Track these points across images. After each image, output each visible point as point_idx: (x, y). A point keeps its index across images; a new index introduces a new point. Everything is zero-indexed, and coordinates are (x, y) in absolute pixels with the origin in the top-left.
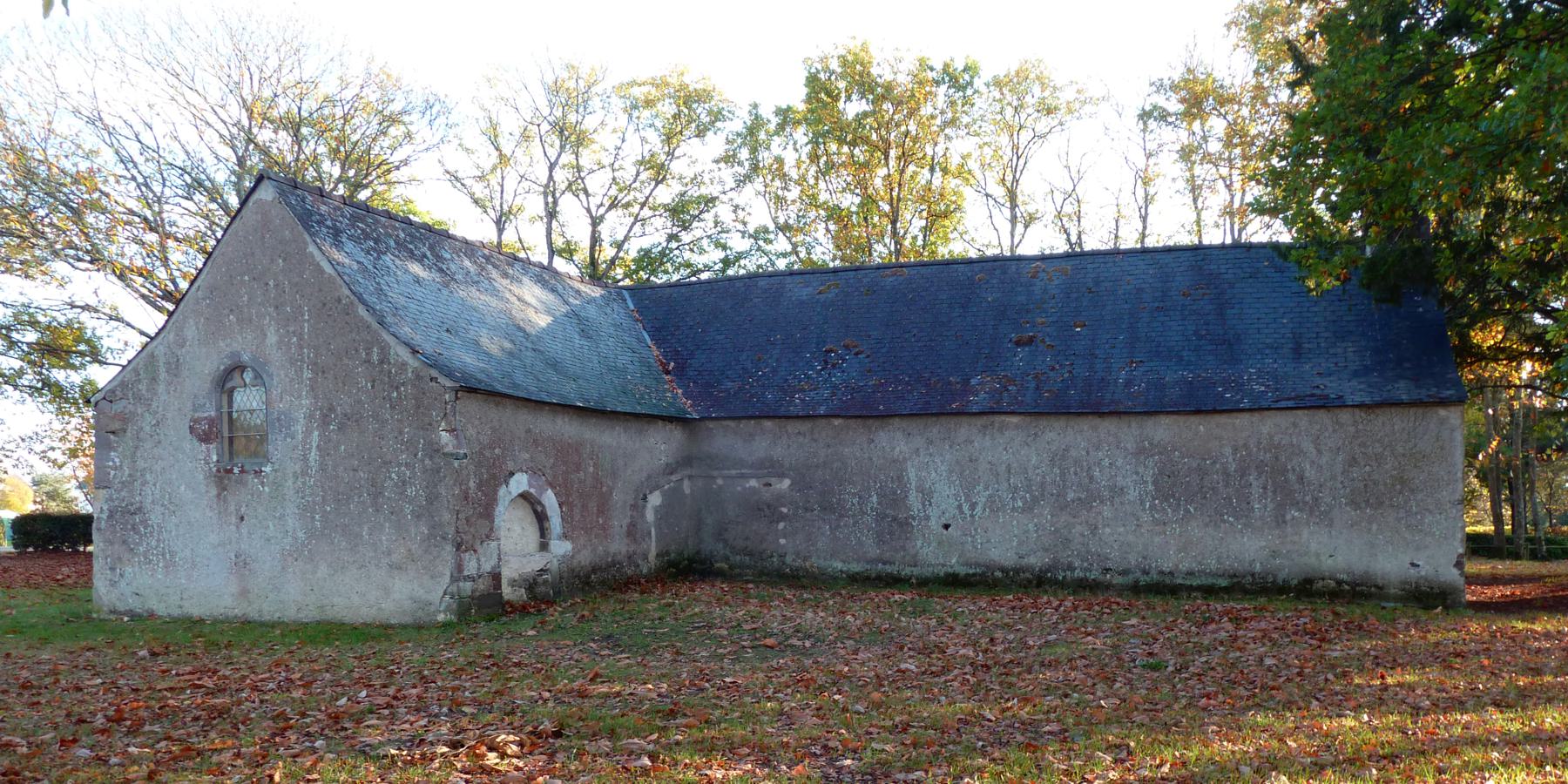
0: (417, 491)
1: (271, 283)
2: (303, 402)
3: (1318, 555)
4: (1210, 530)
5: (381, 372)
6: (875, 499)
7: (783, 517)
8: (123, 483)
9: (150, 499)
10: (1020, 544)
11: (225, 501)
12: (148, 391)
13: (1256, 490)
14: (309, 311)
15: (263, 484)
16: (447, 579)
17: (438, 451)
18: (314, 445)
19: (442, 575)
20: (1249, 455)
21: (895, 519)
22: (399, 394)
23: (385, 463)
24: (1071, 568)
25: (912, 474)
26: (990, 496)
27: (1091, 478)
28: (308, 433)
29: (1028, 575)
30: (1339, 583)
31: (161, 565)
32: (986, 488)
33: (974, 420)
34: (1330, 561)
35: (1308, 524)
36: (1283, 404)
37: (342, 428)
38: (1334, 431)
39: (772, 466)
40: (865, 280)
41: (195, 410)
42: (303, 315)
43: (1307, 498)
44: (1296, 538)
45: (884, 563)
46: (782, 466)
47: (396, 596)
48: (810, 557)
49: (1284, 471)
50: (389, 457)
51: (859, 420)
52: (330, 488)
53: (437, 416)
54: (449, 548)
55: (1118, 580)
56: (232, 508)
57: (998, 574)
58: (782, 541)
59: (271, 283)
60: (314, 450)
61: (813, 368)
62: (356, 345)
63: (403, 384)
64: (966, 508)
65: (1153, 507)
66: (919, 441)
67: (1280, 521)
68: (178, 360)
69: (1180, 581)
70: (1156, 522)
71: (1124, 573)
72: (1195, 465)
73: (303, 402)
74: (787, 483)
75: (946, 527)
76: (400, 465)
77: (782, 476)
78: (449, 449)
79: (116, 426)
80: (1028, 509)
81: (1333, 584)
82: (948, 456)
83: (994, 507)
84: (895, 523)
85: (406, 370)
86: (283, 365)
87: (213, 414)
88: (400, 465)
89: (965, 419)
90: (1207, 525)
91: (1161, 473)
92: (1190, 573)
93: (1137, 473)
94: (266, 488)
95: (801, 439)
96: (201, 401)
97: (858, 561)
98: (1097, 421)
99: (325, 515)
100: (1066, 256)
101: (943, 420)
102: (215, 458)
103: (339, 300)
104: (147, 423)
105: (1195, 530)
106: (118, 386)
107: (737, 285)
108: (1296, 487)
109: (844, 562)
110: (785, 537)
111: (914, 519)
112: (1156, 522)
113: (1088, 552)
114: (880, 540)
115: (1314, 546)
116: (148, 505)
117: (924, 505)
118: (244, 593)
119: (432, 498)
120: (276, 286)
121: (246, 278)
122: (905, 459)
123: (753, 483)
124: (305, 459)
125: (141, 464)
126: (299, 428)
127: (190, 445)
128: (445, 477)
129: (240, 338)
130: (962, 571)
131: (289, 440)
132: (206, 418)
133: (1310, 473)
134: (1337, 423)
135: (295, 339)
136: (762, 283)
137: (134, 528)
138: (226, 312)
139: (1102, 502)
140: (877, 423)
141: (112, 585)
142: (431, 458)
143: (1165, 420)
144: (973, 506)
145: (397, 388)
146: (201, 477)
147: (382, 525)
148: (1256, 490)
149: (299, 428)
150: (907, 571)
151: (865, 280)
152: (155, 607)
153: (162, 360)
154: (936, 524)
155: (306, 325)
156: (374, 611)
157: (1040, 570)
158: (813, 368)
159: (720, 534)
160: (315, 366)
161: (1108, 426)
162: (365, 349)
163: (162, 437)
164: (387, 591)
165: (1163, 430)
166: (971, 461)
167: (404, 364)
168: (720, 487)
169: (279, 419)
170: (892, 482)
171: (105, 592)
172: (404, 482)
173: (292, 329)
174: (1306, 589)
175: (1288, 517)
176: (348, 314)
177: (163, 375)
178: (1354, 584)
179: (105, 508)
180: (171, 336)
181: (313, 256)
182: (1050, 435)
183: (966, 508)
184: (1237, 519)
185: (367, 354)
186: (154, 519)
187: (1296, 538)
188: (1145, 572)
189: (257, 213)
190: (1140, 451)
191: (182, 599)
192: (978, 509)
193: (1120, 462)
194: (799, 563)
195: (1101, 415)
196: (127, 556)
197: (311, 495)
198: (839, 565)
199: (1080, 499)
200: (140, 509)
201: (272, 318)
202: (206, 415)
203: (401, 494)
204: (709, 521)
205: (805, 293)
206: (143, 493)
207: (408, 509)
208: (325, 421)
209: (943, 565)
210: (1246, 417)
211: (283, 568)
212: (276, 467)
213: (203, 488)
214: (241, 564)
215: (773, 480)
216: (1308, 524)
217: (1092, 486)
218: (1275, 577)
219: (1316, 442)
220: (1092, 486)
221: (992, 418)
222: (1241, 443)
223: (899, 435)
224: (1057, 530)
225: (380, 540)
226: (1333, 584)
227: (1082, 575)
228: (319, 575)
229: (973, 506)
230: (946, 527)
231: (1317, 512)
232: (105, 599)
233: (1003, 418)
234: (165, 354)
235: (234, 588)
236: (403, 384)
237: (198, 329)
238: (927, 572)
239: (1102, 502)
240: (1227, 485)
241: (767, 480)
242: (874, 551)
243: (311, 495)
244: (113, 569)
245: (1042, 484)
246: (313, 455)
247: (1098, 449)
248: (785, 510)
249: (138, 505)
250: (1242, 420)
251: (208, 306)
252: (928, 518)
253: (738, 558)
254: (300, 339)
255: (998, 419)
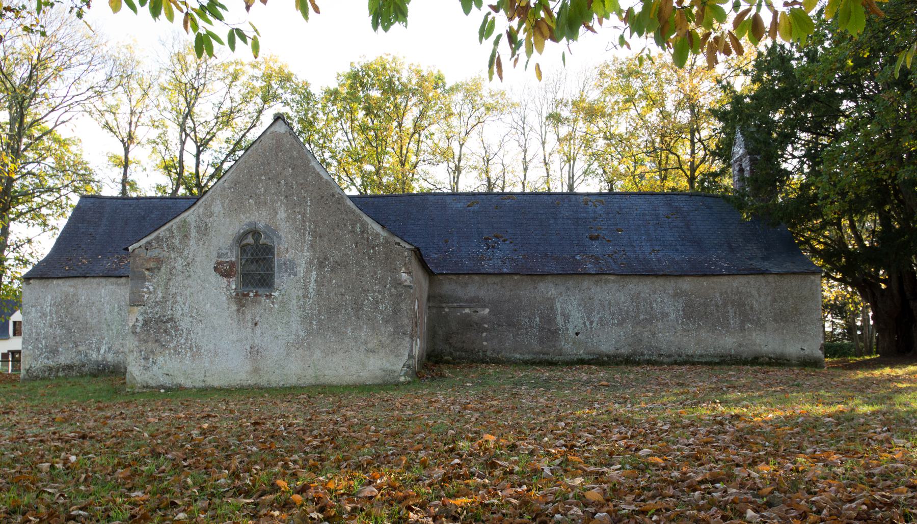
0: (386, 307)
1: (283, 182)
2: (305, 254)
3: (760, 346)
4: (710, 334)
5: (362, 238)
6: (538, 319)
7: (485, 330)
8: (157, 302)
9: (180, 312)
10: (617, 342)
11: (243, 313)
12: (180, 243)
13: (731, 314)
14: (310, 200)
15: (273, 303)
16: (406, 357)
17: (400, 284)
18: (313, 280)
19: (402, 355)
20: (728, 297)
21: (549, 330)
22: (374, 251)
23: (364, 291)
24: (643, 354)
25: (558, 305)
26: (600, 318)
27: (652, 308)
28: (308, 272)
29: (620, 359)
30: (770, 358)
31: (188, 355)
32: (598, 313)
33: (591, 277)
34: (765, 349)
35: (755, 330)
36: (741, 272)
37: (333, 270)
38: (766, 286)
39: (478, 302)
40: (493, 201)
41: (219, 256)
42: (307, 202)
43: (755, 318)
44: (750, 337)
45: (544, 354)
46: (484, 301)
47: (371, 368)
48: (501, 352)
49: (744, 305)
50: (366, 287)
51: (529, 277)
52: (324, 305)
53: (400, 264)
54: (408, 339)
55: (666, 360)
56: (249, 317)
57: (606, 359)
58: (485, 343)
59: (283, 182)
60: (312, 282)
61: (482, 248)
62: (345, 221)
63: (377, 246)
64: (587, 324)
65: (682, 323)
66: (562, 288)
67: (742, 329)
68: (206, 225)
69: (696, 360)
70: (684, 330)
71: (670, 356)
72: (702, 301)
73: (305, 254)
74: (487, 310)
75: (577, 334)
76: (374, 292)
77: (484, 307)
78: (408, 283)
79: (152, 265)
80: (620, 324)
81: (767, 359)
82: (578, 297)
83: (603, 323)
84: (550, 332)
85: (379, 238)
86: (290, 232)
87: (233, 259)
88: (374, 292)
89: (586, 277)
90: (709, 332)
91: (686, 305)
92: (701, 356)
93: (675, 306)
94: (276, 306)
95: (495, 286)
96: (224, 251)
97: (529, 353)
98: (654, 279)
99: (320, 322)
100: (691, 195)
101: (575, 277)
102: (234, 287)
103: (333, 195)
104: (179, 264)
105: (703, 334)
106: (154, 239)
107: (416, 199)
108: (750, 312)
109: (521, 354)
110: (486, 341)
111: (560, 330)
112: (684, 330)
113: (651, 346)
114: (541, 342)
115: (758, 341)
116: (178, 315)
117: (565, 323)
118: (256, 371)
119: (396, 311)
120: (286, 184)
121: (263, 178)
122: (554, 298)
123: (467, 311)
124: (306, 288)
125: (173, 290)
126: (301, 270)
127: (214, 277)
128: (405, 299)
129: (257, 214)
130: (586, 357)
131: (292, 276)
132: (228, 262)
133: (756, 305)
134: (767, 282)
135: (300, 216)
136: (432, 198)
137: (165, 331)
138: (247, 197)
139: (657, 320)
140: (539, 278)
141: (145, 370)
142: (395, 288)
143: (688, 279)
144: (591, 323)
145: (373, 248)
146: (224, 298)
147: (361, 327)
148: (731, 314)
149: (301, 270)
150: (556, 358)
151: (493, 201)
152: (182, 383)
153: (193, 224)
154: (571, 332)
155: (308, 208)
156: (354, 377)
157: (627, 356)
158: (482, 248)
159: (447, 340)
160: (314, 234)
161: (659, 282)
162: (351, 225)
163: (192, 273)
164: (364, 365)
165: (686, 284)
166: (590, 299)
167: (378, 234)
168: (446, 313)
169: (285, 264)
170: (548, 310)
171: (138, 374)
172: (377, 302)
173: (297, 210)
174: (756, 361)
175: (746, 327)
176: (339, 204)
177: (193, 233)
178: (777, 359)
179: (140, 318)
180: (201, 210)
181: (314, 168)
182: (631, 286)
183: (587, 324)
184: (723, 328)
185: (352, 227)
186: (184, 324)
187: (750, 337)
188: (680, 356)
189: (272, 139)
190: (676, 295)
191: (205, 376)
192: (594, 324)
193: (666, 300)
194: (494, 355)
195: (656, 276)
196: (159, 349)
197: (310, 309)
198: (518, 356)
199: (646, 319)
200: (171, 319)
201: (282, 203)
202: (228, 260)
203: (375, 308)
204: (440, 332)
205: (459, 206)
206: (174, 309)
207: (379, 317)
208: (321, 265)
209: (576, 355)
210: (726, 278)
211: (287, 354)
212: (283, 292)
213: (225, 306)
214: (255, 352)
215: (479, 309)
216: (755, 330)
217: (652, 312)
218: (741, 356)
219: (758, 290)
220: (652, 312)
221: (600, 277)
222: (724, 291)
223: (551, 285)
224: (635, 335)
225: (360, 336)
226: (767, 359)
227: (648, 358)
228: (315, 357)
229: (591, 323)
230: (577, 334)
231: (760, 326)
232: (139, 379)
233: (606, 277)
234: (196, 221)
235: (248, 367)
236: (377, 246)
237: (223, 207)
238: (567, 358)
239: (657, 320)
240: (718, 312)
241: (475, 309)
242: (538, 348)
243: (310, 309)
244: (146, 359)
245: (627, 312)
246: (312, 286)
247: (655, 293)
248: (486, 326)
249: (169, 317)
250: (724, 280)
251: (232, 193)
252: (567, 329)
253: (458, 353)
254: (304, 215)
255: (604, 277)
